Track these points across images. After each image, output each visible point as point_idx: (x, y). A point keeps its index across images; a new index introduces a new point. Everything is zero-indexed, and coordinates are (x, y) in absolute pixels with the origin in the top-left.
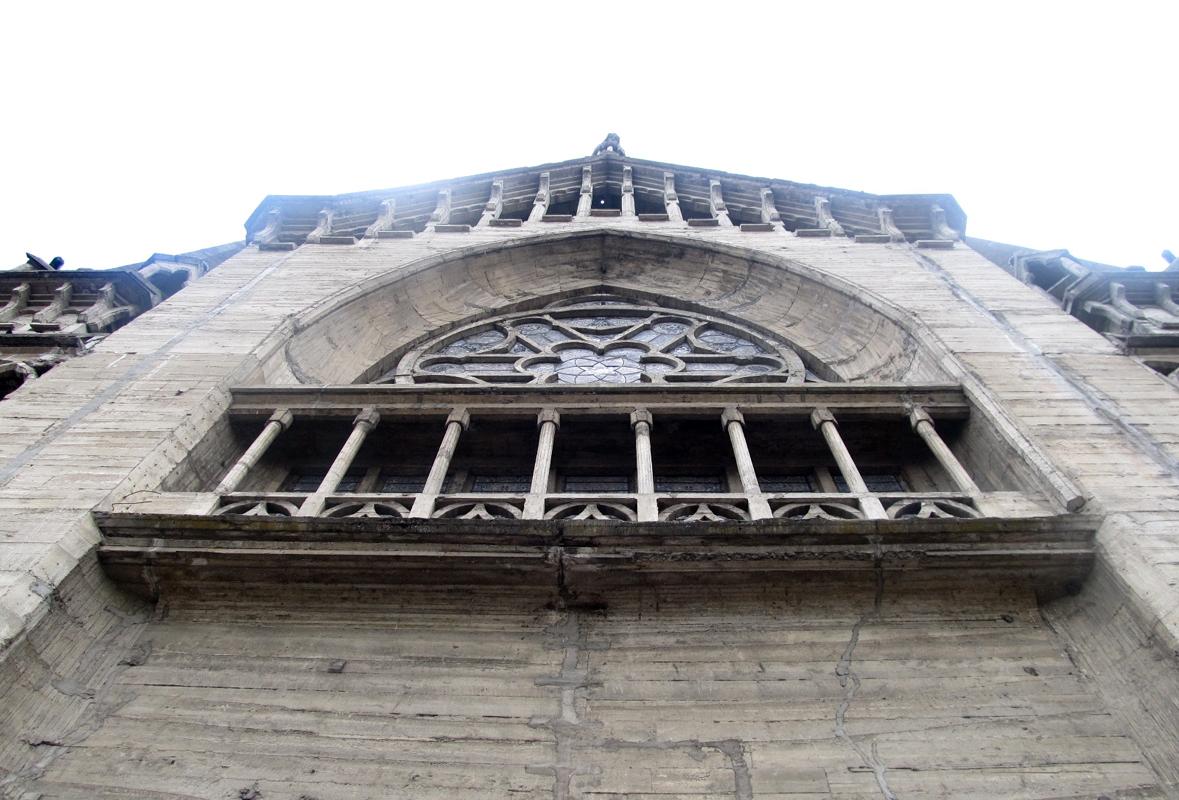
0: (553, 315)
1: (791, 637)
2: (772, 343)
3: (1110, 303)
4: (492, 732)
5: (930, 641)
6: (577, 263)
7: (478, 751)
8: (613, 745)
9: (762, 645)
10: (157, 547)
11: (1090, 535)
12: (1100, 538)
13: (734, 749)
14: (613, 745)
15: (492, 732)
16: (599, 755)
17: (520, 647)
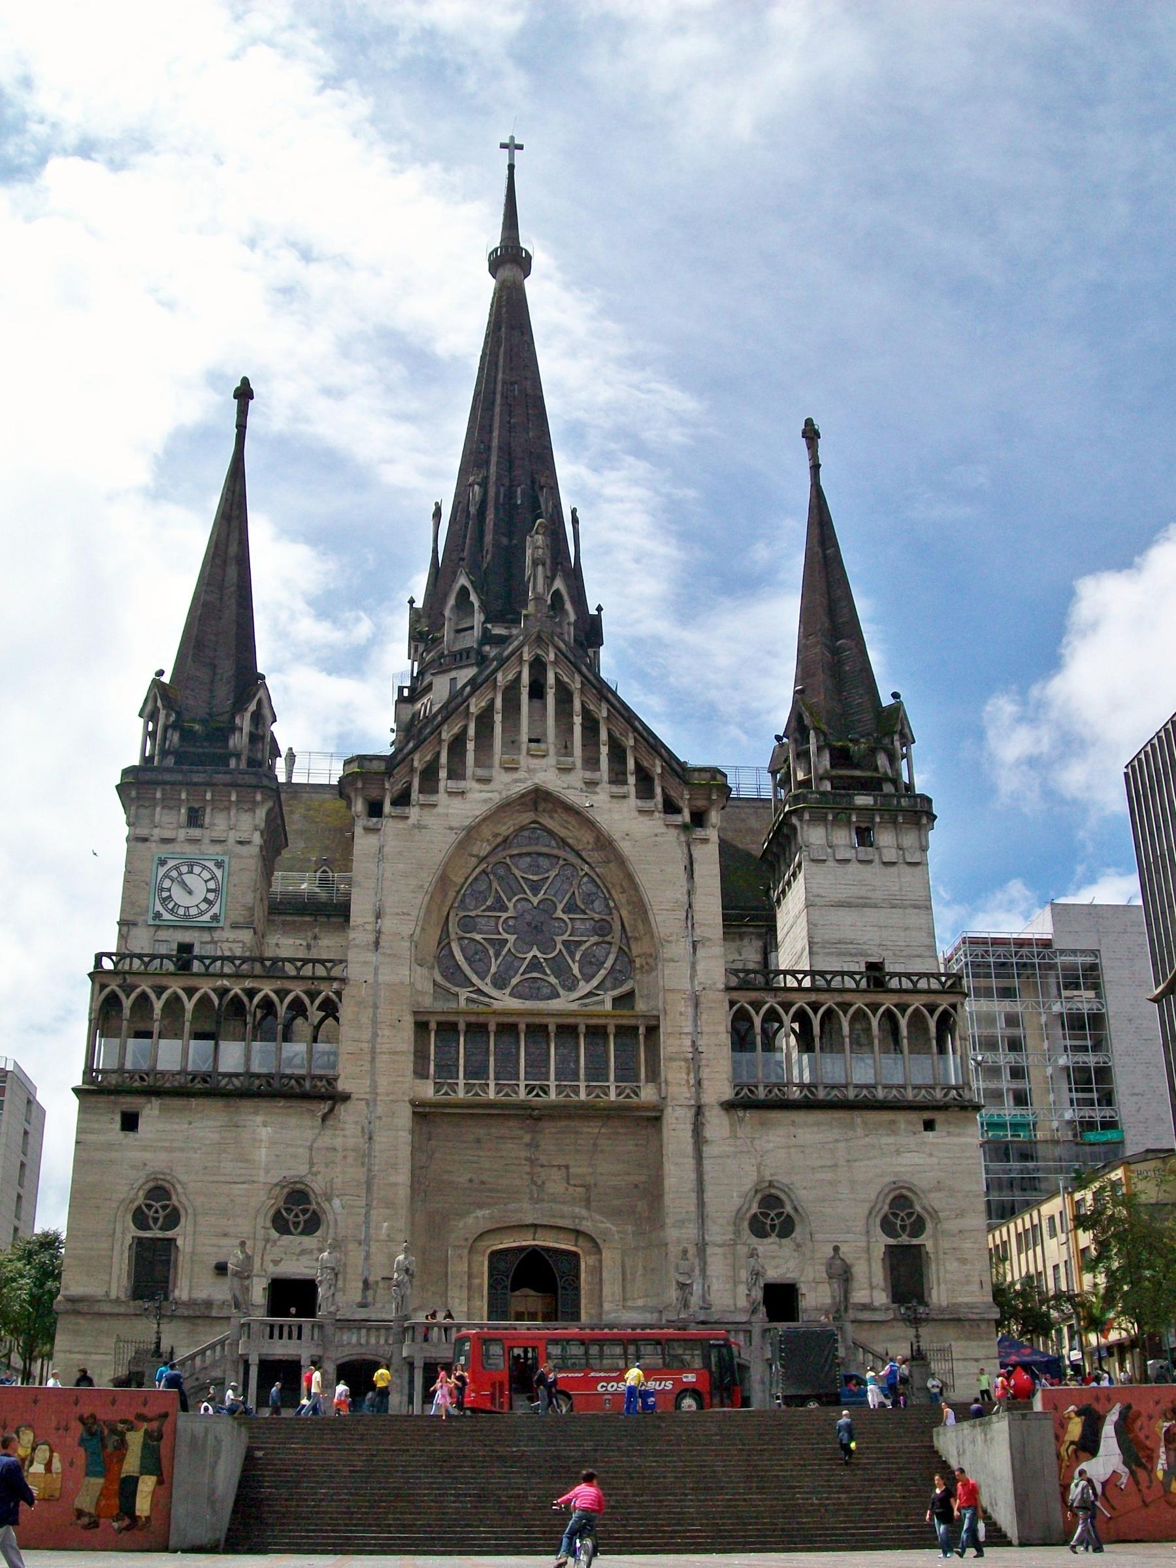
0: (511, 856)
1: (585, 1130)
2: (612, 904)
3: (801, 820)
4: (516, 1162)
5: (618, 1133)
6: (522, 804)
7: (513, 1167)
8: (542, 1166)
9: (577, 1133)
10: (427, 1110)
11: (662, 1111)
12: (665, 1112)
13: (567, 1167)
14: (542, 1166)
15: (516, 1162)
16: (540, 1169)
17: (520, 1132)
